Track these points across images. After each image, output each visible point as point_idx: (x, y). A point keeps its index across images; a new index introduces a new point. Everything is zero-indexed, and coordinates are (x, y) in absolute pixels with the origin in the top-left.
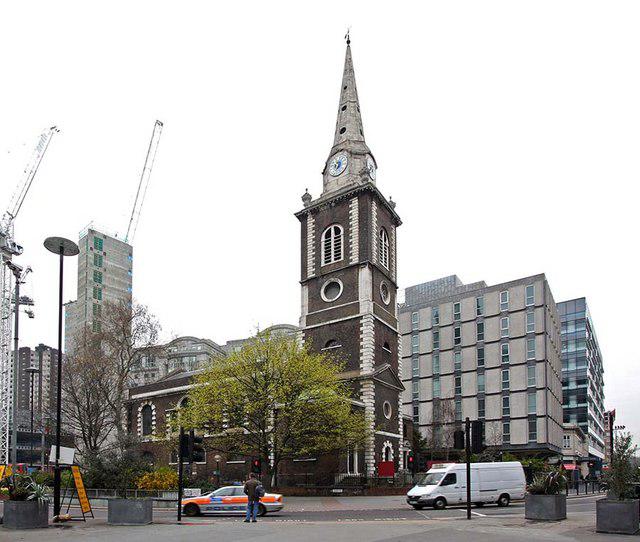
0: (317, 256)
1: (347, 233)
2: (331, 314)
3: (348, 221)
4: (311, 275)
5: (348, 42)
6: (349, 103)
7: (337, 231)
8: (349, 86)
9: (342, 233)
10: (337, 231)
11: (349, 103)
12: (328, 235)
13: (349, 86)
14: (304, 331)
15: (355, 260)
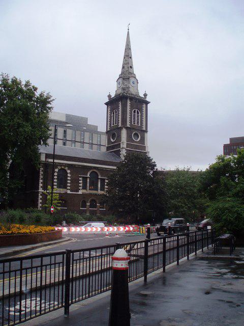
0: (131, 118)
1: (142, 116)
2: (137, 147)
3: (127, 104)
4: (128, 125)
5: (128, 30)
6: (128, 56)
7: (138, 113)
8: (128, 48)
9: (140, 114)
10: (138, 113)
11: (128, 56)
12: (135, 112)
13: (128, 48)
14: (126, 150)
15: (144, 129)
